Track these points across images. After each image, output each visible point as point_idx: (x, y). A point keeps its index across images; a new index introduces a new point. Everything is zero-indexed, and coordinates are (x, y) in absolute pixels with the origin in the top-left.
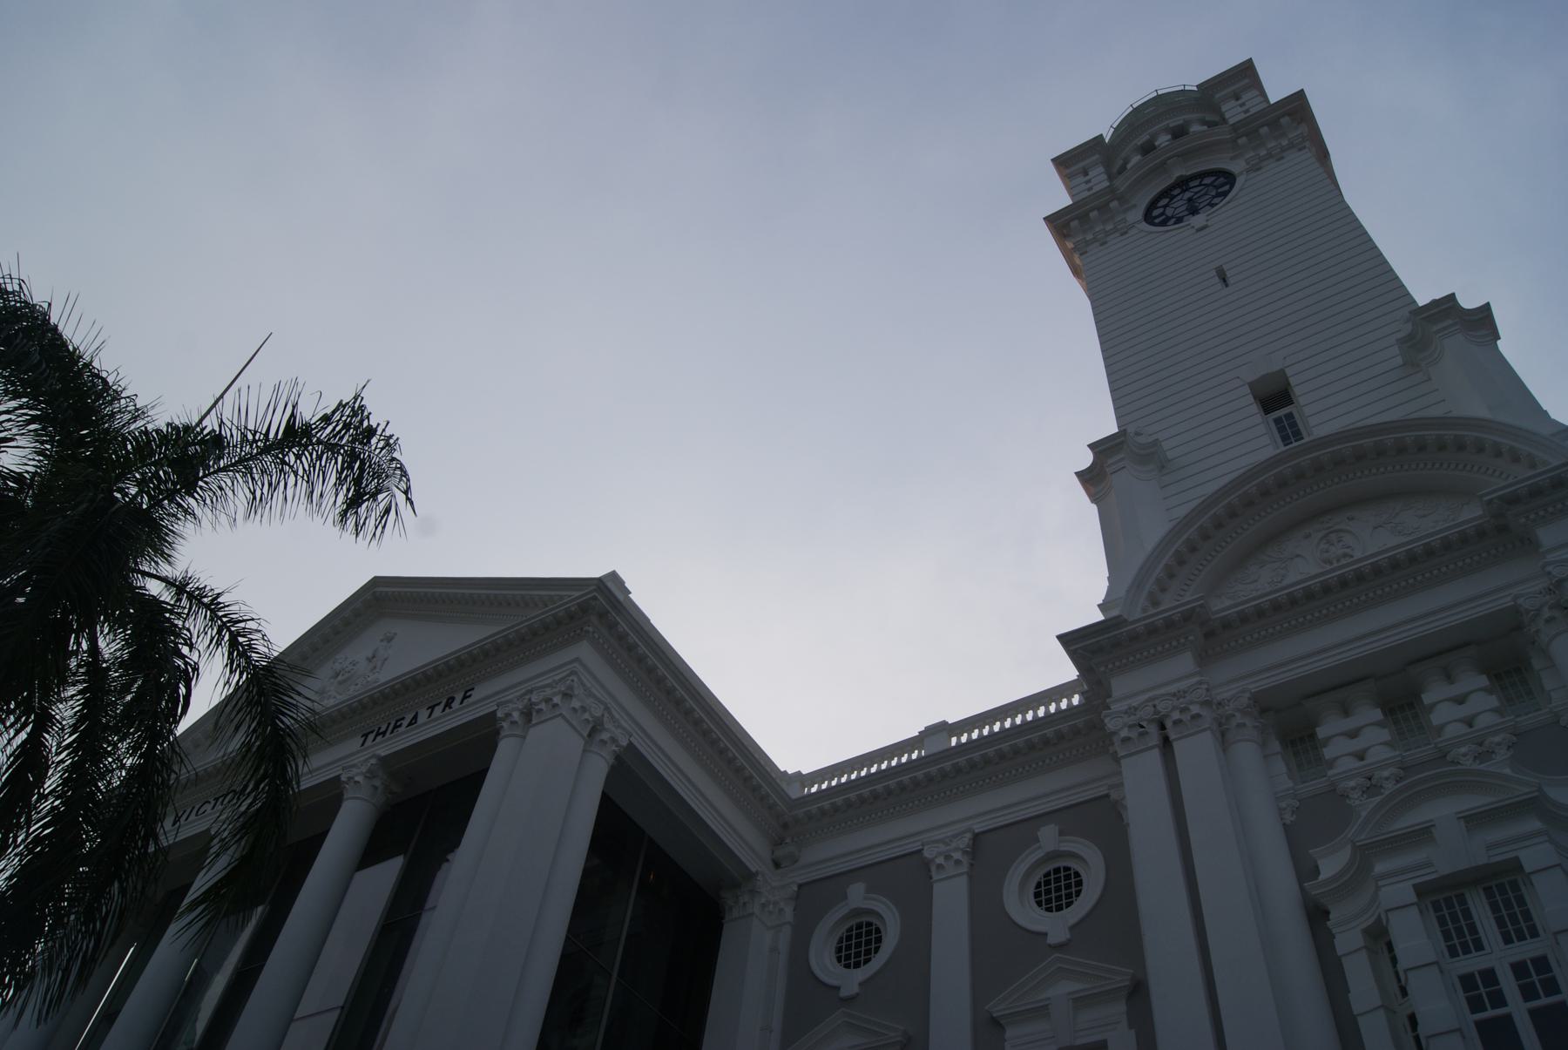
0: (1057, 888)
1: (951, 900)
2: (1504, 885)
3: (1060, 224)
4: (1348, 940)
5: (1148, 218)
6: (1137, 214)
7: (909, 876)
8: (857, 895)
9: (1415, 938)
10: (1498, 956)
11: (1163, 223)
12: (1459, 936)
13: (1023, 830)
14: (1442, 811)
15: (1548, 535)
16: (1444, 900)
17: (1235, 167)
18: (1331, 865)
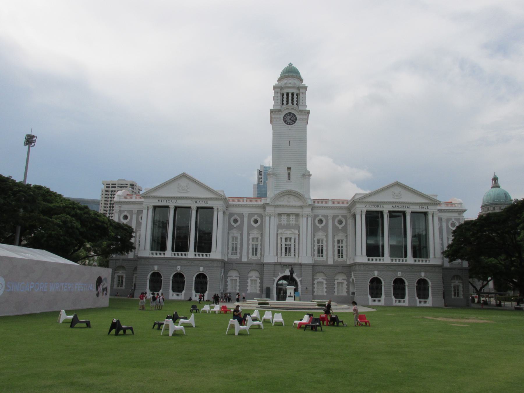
0: (256, 221)
1: (246, 220)
2: (290, 239)
3: (272, 111)
4: (279, 238)
5: (284, 119)
6: (282, 117)
7: (242, 215)
8: (236, 216)
9: (284, 240)
10: (288, 243)
11: (285, 122)
12: (286, 241)
13: (253, 215)
14: (289, 232)
15: (305, 209)
16: (286, 239)
17: (297, 116)
18: (280, 231)
